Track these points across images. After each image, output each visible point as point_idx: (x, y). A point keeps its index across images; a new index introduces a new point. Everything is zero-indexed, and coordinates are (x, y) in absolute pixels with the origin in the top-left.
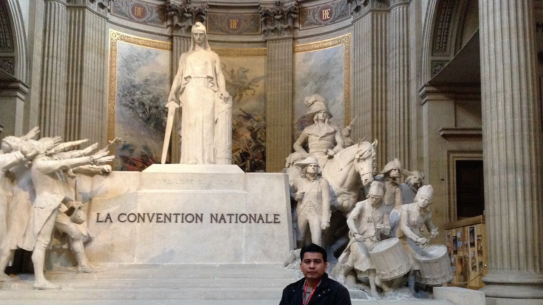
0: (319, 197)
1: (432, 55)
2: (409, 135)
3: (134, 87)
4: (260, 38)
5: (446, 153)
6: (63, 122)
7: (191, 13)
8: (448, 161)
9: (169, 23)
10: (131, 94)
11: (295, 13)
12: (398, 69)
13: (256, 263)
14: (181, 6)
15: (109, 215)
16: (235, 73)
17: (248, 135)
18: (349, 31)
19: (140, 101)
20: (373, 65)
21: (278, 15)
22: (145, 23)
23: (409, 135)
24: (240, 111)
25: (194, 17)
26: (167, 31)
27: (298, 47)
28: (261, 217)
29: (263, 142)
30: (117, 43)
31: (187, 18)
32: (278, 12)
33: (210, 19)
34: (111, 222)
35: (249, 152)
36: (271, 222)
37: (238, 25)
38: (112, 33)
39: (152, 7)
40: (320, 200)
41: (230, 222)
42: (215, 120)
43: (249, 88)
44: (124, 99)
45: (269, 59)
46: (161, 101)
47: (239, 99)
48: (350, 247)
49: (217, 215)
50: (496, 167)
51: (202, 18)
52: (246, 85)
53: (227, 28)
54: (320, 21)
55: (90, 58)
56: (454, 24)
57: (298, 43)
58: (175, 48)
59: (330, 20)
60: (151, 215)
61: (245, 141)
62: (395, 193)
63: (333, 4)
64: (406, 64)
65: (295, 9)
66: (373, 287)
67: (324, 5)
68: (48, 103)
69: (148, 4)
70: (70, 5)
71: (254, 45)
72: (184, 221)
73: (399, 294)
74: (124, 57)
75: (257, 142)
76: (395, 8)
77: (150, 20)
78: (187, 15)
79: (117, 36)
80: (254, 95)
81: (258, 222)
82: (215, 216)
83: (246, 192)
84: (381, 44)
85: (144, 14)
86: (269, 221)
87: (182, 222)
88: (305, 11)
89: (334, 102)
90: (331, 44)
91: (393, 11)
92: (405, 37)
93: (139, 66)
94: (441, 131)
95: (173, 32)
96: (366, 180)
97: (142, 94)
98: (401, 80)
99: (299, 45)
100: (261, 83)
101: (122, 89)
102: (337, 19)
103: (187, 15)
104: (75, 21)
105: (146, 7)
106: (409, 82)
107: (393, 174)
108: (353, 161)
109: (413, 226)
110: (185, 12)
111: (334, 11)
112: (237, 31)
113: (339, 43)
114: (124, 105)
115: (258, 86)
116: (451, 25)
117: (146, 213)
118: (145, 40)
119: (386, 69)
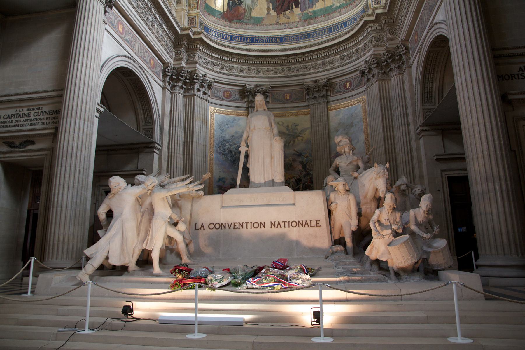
1: (423, 105)
3: (225, 141)
10: (223, 145)
11: (327, 86)
12: (400, 117)
13: (304, 256)
15: (202, 224)
16: (290, 127)
17: (300, 167)
21: (316, 88)
22: (231, 101)
26: (245, 105)
29: (311, 171)
33: (272, 95)
34: (204, 229)
35: (301, 178)
37: (291, 97)
41: (285, 227)
43: (299, 136)
55: (197, 126)
57: (331, 104)
60: (230, 224)
62: (405, 201)
72: (252, 227)
73: (412, 278)
75: (306, 171)
85: (230, 95)
89: (358, 142)
91: (393, 80)
97: (230, 145)
98: (403, 123)
99: (331, 106)
100: (308, 132)
106: (408, 124)
107: (403, 187)
108: (372, 179)
111: (353, 83)
114: (220, 153)
119: (392, 117)
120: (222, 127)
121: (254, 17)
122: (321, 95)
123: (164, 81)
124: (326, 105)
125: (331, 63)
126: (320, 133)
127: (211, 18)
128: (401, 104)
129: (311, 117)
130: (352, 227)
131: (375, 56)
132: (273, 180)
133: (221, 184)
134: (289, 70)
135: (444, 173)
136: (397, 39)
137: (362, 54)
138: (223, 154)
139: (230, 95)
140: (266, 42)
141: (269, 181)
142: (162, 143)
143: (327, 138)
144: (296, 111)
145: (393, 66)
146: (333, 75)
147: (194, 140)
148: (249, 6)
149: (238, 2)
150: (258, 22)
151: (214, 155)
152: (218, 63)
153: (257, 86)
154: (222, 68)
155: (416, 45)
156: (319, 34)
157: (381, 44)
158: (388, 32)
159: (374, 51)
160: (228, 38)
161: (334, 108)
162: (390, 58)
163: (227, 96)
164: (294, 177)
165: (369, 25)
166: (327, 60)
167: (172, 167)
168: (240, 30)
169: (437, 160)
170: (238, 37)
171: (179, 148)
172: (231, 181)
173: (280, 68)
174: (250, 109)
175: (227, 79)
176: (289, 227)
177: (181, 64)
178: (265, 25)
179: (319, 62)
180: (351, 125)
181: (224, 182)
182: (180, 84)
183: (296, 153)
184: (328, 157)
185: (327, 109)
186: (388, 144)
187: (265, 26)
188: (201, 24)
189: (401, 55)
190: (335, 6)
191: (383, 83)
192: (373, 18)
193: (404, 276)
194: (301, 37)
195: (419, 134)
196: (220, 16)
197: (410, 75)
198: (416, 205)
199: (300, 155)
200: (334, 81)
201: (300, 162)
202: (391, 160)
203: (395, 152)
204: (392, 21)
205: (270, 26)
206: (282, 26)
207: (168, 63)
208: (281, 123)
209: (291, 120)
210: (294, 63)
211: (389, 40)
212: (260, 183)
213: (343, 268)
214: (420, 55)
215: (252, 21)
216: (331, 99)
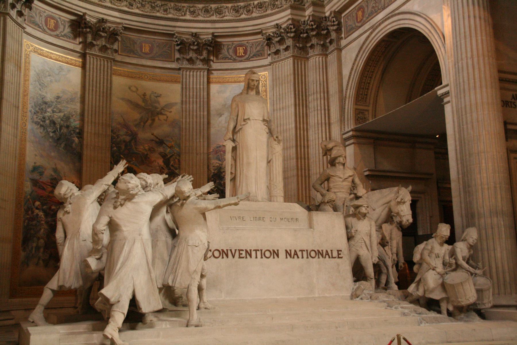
1: (356, 104)
3: (46, 103)
4: (174, 65)
7: (106, 32)
9: (81, 40)
11: (210, 46)
12: (319, 112)
13: (327, 295)
14: (96, 24)
16: (148, 97)
18: (265, 71)
19: (51, 119)
21: (194, 45)
22: (57, 36)
24: (152, 136)
25: (108, 37)
26: (78, 48)
29: (176, 169)
30: (31, 55)
31: (101, 37)
32: (194, 43)
36: (335, 258)
37: (151, 49)
38: (26, 43)
39: (64, 21)
40: (369, 237)
41: (303, 257)
42: (269, 159)
43: (161, 114)
44: (35, 116)
46: (72, 120)
47: (151, 125)
48: (420, 280)
49: (290, 251)
51: (116, 38)
52: (158, 110)
53: (139, 51)
54: (235, 57)
58: (88, 66)
59: (245, 58)
60: (233, 252)
61: (158, 168)
63: (247, 43)
64: (326, 108)
65: (211, 43)
67: (238, 43)
69: (62, 18)
71: (132, 66)
74: (37, 70)
75: (170, 169)
76: (315, 57)
77: (63, 34)
78: (103, 34)
79: (31, 48)
80: (166, 120)
81: (325, 258)
82: (289, 252)
83: (312, 230)
85: (56, 27)
86: (334, 256)
87: (262, 258)
92: (325, 83)
94: (364, 172)
95: (85, 50)
97: (53, 112)
98: (323, 121)
101: (33, 104)
102: (252, 57)
103: (103, 34)
105: (59, 20)
108: (388, 203)
110: (100, 30)
111: (249, 49)
112: (151, 56)
114: (37, 123)
117: (229, 249)
118: (57, 55)
119: (306, 110)
122: (202, 58)
124: (206, 73)
125: (219, 11)
126: (195, 114)
128: (322, 95)
129: (182, 88)
131: (295, 23)
133: (36, 176)
134: (152, 6)
137: (269, 12)
138: (41, 126)
139: (56, 27)
143: (206, 123)
145: (314, 41)
151: (29, 126)
153: (102, 21)
155: (359, 25)
159: (291, 14)
162: (313, 30)
172: (53, 174)
181: (41, 174)
183: (155, 139)
184: (206, 151)
186: (301, 146)
189: (328, 29)
195: (346, 139)
199: (160, 142)
201: (160, 154)
202: (303, 167)
203: (308, 158)
208: (134, 89)
214: (366, 40)
216: (214, 66)
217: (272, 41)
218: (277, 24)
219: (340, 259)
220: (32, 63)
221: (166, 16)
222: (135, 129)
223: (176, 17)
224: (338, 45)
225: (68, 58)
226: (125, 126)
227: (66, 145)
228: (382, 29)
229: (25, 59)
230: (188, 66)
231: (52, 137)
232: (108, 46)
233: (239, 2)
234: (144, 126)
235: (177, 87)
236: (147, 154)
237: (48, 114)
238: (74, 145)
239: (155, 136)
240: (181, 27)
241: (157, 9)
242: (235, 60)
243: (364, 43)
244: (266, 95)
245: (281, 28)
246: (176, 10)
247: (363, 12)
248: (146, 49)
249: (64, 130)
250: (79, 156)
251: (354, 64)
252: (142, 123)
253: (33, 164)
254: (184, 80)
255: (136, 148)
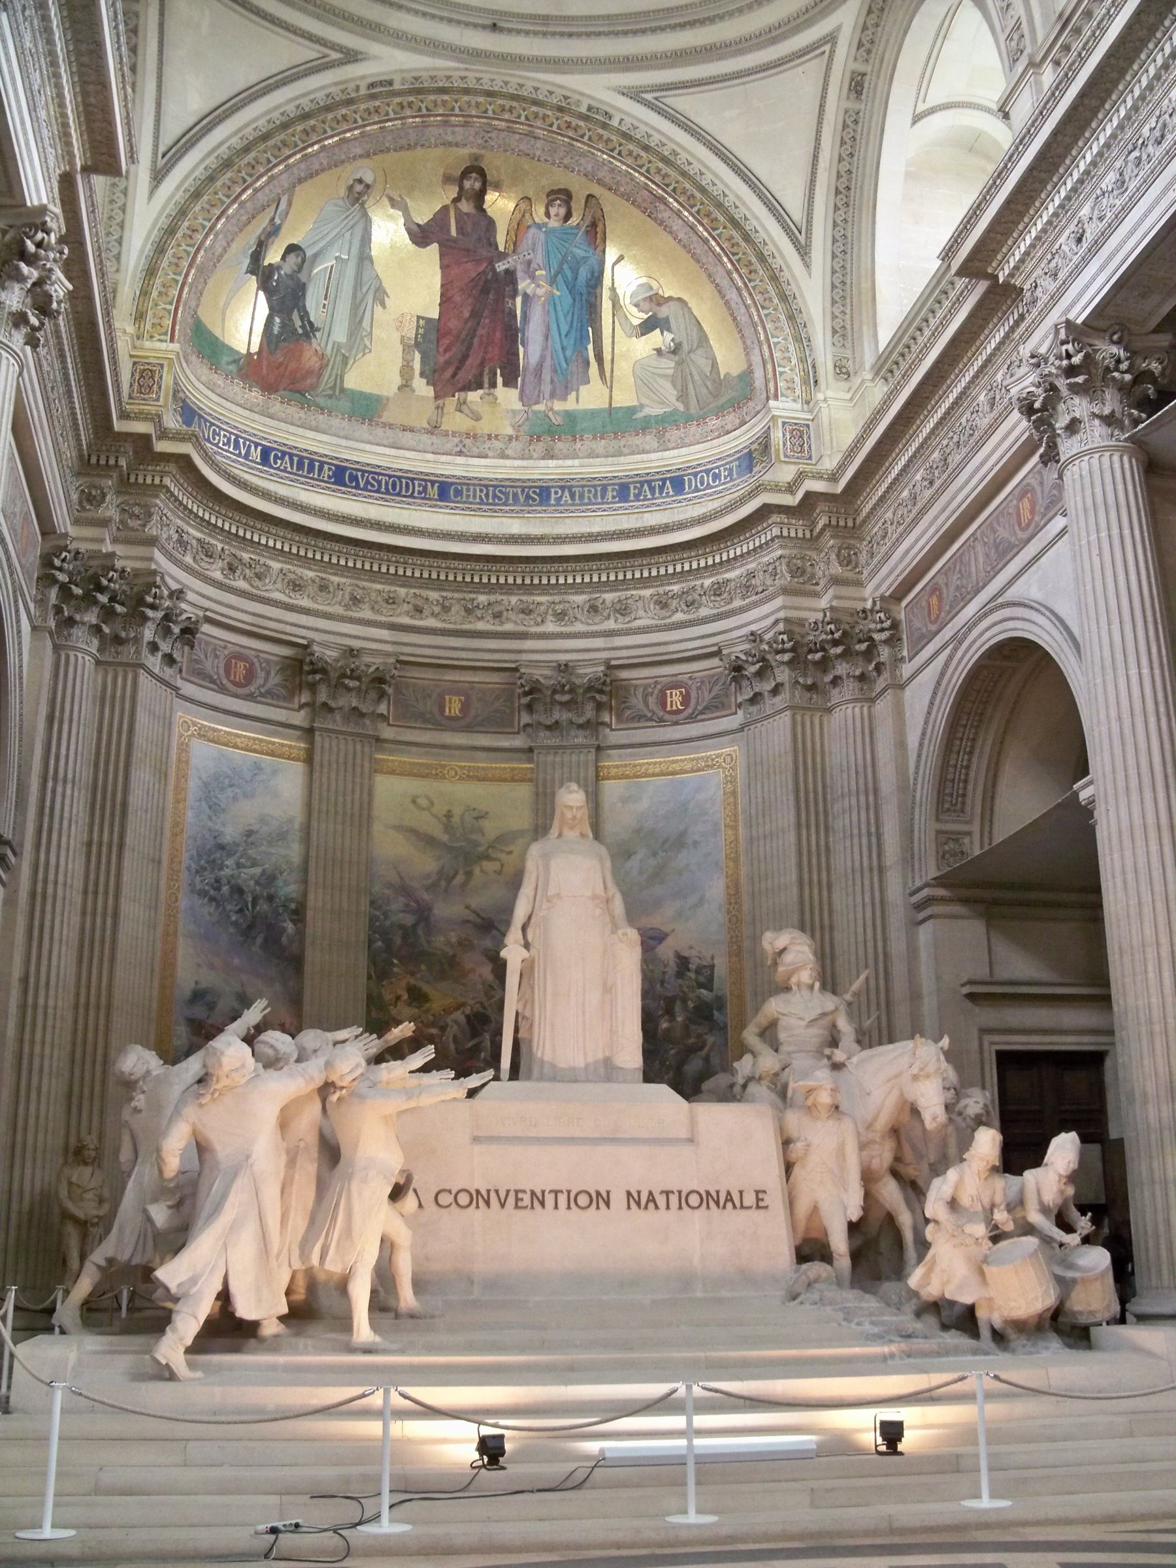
0: (841, 1152)
1: (937, 819)
2: (887, 990)
3: (222, 847)
4: (519, 742)
5: (975, 1035)
6: (74, 936)
7: (358, 679)
8: (981, 1051)
9: (305, 698)
11: (601, 692)
12: (856, 841)
14: (337, 661)
16: (456, 819)
20: (799, 825)
21: (563, 692)
22: (250, 697)
23: (887, 990)
27: (609, 767)
28: (729, 1197)
31: (349, 689)
33: (397, 689)
37: (465, 708)
39: (268, 662)
41: (668, 1207)
43: (487, 857)
44: (198, 879)
45: (541, 790)
46: (280, 882)
49: (639, 1193)
50: (1150, 1089)
52: (481, 849)
54: (661, 713)
56: (980, 758)
58: (317, 758)
59: (686, 714)
60: (502, 1195)
61: (480, 986)
64: (873, 830)
65: (604, 683)
66: (985, 1333)
68: (50, 891)
70: (105, 658)
74: (204, 776)
78: (352, 684)
84: (806, 780)
85: (250, 675)
87: (569, 1207)
88: (626, 689)
89: (701, 902)
90: (689, 766)
91: (837, 715)
93: (235, 798)
95: (313, 721)
96: (934, 1119)
97: (239, 865)
98: (865, 864)
99: (612, 762)
101: (194, 852)
102: (701, 713)
104: (113, 696)
106: (881, 870)
109: (1044, 1210)
110: (344, 676)
111: (693, 694)
113: (712, 767)
114: (202, 893)
115: (511, 852)
116: (975, 759)
120: (217, 792)
121: (353, 392)
122: (581, 721)
123: (41, 602)
125: (622, 610)
127: (205, 372)
128: (862, 798)
129: (537, 794)
130: (849, 1212)
132: (608, 1063)
133: (199, 1012)
134: (469, 611)
135: (987, 1038)
136: (859, 584)
137: (737, 603)
138: (212, 899)
139: (250, 675)
140: (387, 492)
141: (596, 1062)
142: (22, 845)
144: (482, 763)
145: (841, 669)
146: (624, 653)
147: (129, 840)
148: (338, 347)
149: (303, 327)
150: (366, 409)
152: (220, 546)
153: (352, 652)
154: (232, 569)
155: (933, 628)
156: (582, 496)
157: (809, 587)
158: (833, 557)
159: (784, 607)
160: (256, 454)
161: (620, 771)
162: (836, 643)
163: (237, 676)
164: (463, 1005)
165: (775, 518)
166: (609, 597)
167: (46, 936)
168: (300, 431)
169: (971, 997)
170: (291, 456)
171: (70, 865)
173: (434, 595)
174: (318, 738)
175: (245, 611)
176: (680, 1208)
177: (102, 541)
178: (391, 426)
179: (580, 599)
180: (679, 842)
181: (211, 1007)
182: (91, 617)
183: (472, 917)
185: (597, 772)
187: (389, 433)
188: (176, 392)
189: (871, 639)
190: (647, 411)
191: (807, 718)
192: (793, 500)
193: (1017, 1341)
194: (515, 495)
195: (919, 907)
196: (233, 368)
197: (899, 711)
198: (1037, 1160)
200: (625, 674)
204: (850, 524)
205: (409, 435)
206: (451, 443)
207: (66, 535)
209: (462, 793)
210: (489, 588)
211: (836, 581)
212: (573, 1069)
213: (873, 1323)
214: (947, 665)
215: (344, 404)
216: (614, 737)
217: (742, 676)
218: (752, 634)
219: (762, 1211)
220: (194, 762)
221: (499, 628)
222: (426, 897)
223: (522, 628)
224: (894, 676)
225: (273, 743)
226: (404, 890)
227: (266, 940)
228: (974, 641)
229: (179, 755)
230: (549, 742)
231: (235, 924)
232: (364, 708)
233: (669, 584)
234: (446, 890)
235: (523, 792)
236: (454, 956)
237: (227, 872)
238: (284, 939)
239: (475, 912)
240: (533, 651)
241: (479, 613)
242: (661, 720)
243: (942, 674)
244: (735, 804)
245: (762, 641)
246: (523, 612)
247: (940, 599)
248: (454, 707)
249: (263, 907)
250: (296, 963)
251: (926, 723)
252: (442, 882)
253: (193, 985)
254: (541, 776)
255: (429, 942)
